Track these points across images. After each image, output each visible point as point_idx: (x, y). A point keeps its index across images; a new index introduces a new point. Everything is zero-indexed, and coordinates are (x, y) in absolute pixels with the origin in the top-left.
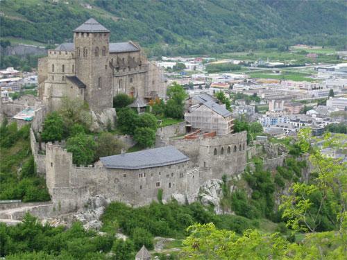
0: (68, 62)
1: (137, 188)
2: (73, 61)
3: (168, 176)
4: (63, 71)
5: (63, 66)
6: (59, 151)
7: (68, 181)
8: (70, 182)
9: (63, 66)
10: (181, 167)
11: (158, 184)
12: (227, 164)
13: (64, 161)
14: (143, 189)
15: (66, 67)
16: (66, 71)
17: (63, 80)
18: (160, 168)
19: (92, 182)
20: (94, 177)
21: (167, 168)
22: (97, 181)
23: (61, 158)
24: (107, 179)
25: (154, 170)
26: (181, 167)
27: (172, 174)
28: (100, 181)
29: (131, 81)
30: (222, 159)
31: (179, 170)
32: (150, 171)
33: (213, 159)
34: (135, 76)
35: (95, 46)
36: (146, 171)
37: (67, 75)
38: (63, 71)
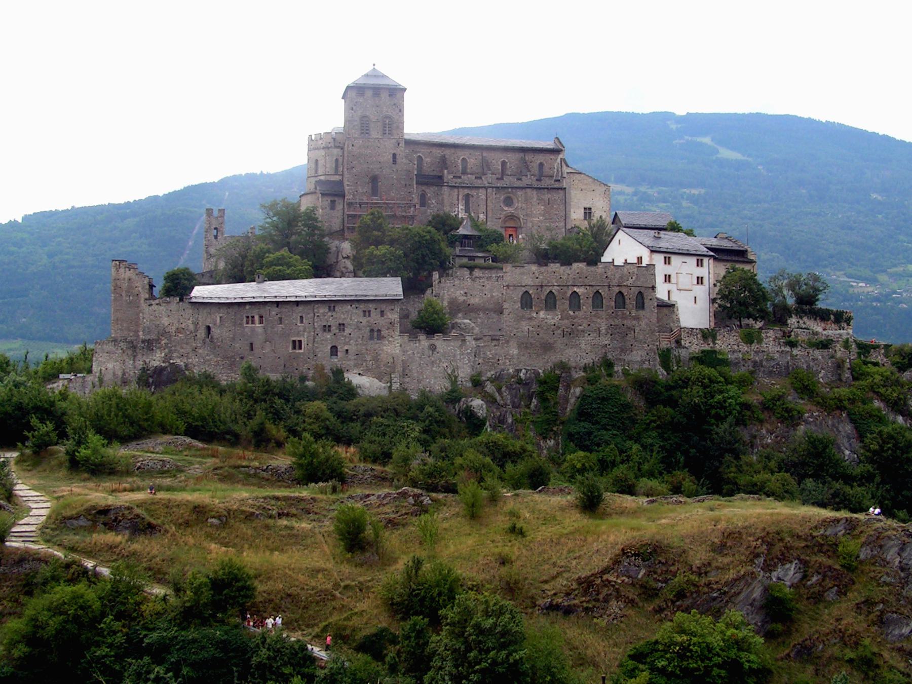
0: (323, 152)
1: (240, 346)
2: (336, 151)
3: (327, 328)
4: (316, 171)
5: (317, 161)
6: (122, 270)
7: (137, 332)
8: (141, 333)
9: (317, 161)
10: (375, 315)
11: (297, 345)
12: (571, 334)
13: (129, 292)
14: (257, 350)
15: (321, 163)
16: (320, 172)
17: (316, 188)
18: (300, 308)
19: (164, 333)
20: (165, 321)
21: (323, 310)
22: (173, 329)
23: (125, 285)
24: (192, 327)
25: (284, 309)
26: (375, 315)
27: (342, 326)
28: (178, 331)
29: (509, 202)
30: (553, 322)
31: (364, 320)
32: (274, 310)
33: (520, 319)
34: (519, 193)
35: (359, 113)
36: (264, 311)
37: (322, 178)
38: (316, 171)
